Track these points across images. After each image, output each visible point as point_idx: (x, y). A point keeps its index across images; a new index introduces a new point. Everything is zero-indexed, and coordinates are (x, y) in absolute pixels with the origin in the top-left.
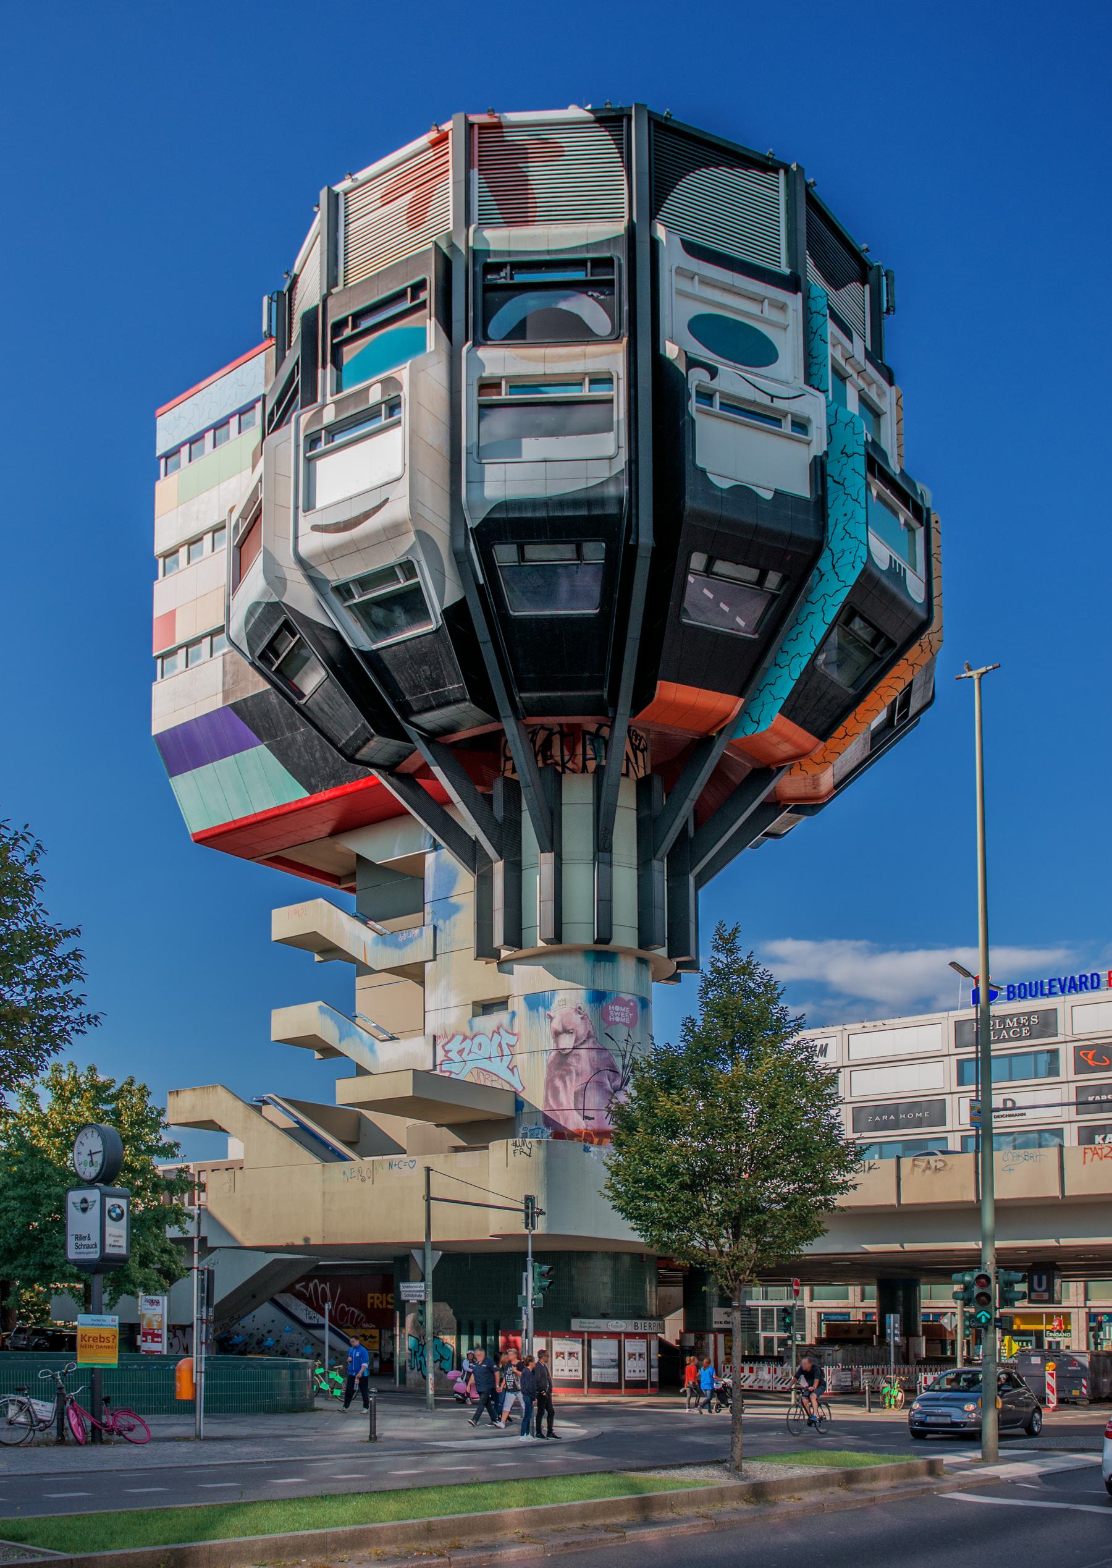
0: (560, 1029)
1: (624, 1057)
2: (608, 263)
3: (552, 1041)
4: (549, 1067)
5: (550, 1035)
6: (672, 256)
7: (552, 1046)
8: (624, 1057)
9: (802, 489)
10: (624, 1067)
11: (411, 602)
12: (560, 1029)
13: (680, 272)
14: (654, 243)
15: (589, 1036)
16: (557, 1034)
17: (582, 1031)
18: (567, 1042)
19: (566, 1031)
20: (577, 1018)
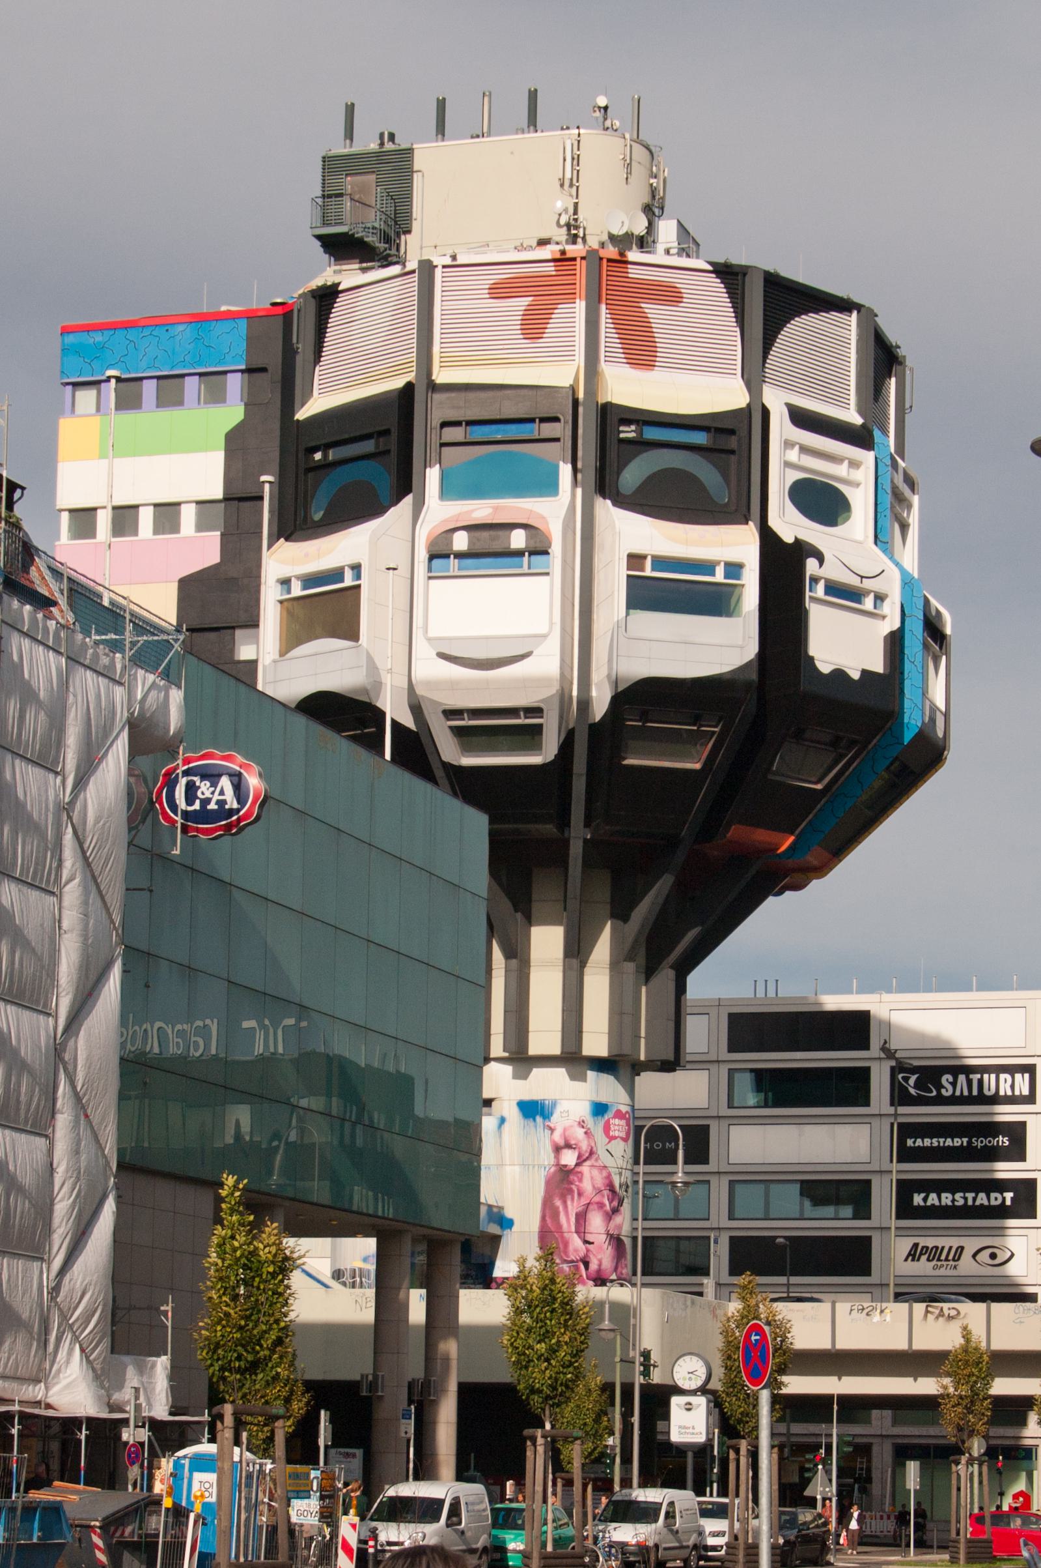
0: (562, 1143)
1: (620, 1174)
2: (732, 432)
3: (552, 1155)
4: (548, 1183)
5: (549, 1148)
6: (780, 427)
7: (552, 1161)
8: (620, 1174)
9: (877, 665)
10: (621, 1186)
11: (530, 736)
12: (562, 1143)
13: (788, 444)
14: (766, 413)
15: (592, 1153)
16: (557, 1149)
17: (584, 1146)
18: (569, 1158)
19: (568, 1146)
20: (580, 1133)
